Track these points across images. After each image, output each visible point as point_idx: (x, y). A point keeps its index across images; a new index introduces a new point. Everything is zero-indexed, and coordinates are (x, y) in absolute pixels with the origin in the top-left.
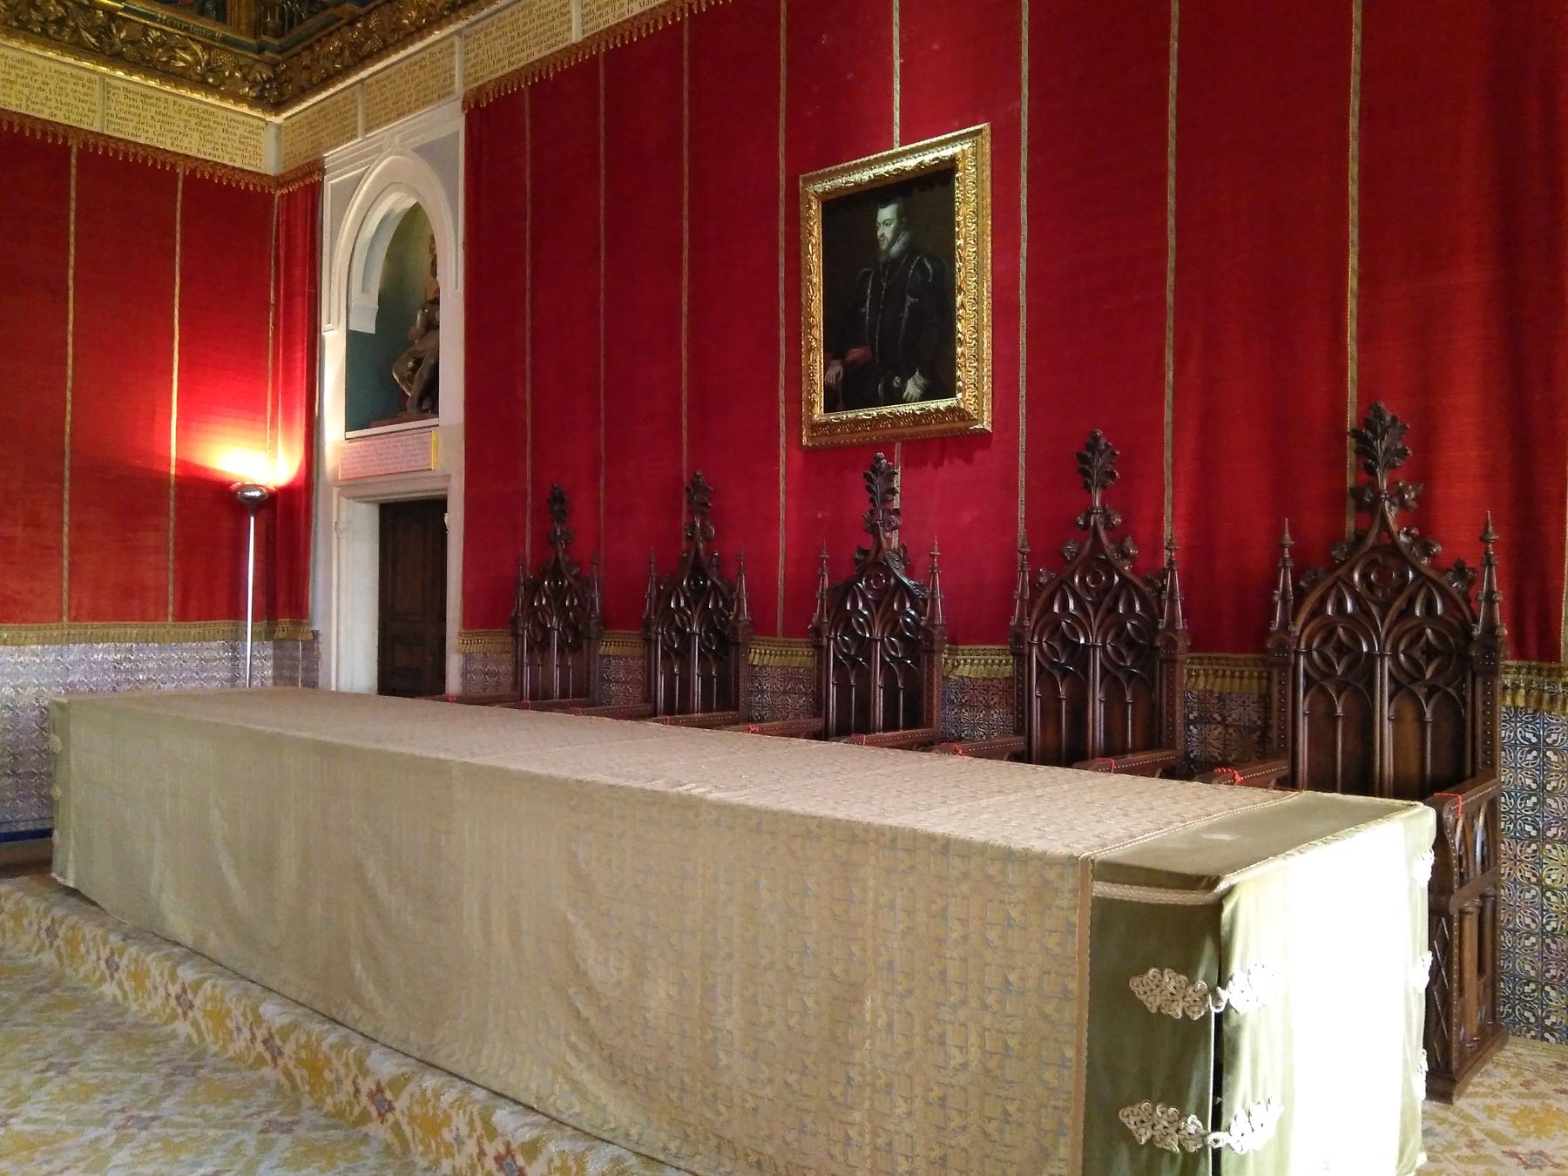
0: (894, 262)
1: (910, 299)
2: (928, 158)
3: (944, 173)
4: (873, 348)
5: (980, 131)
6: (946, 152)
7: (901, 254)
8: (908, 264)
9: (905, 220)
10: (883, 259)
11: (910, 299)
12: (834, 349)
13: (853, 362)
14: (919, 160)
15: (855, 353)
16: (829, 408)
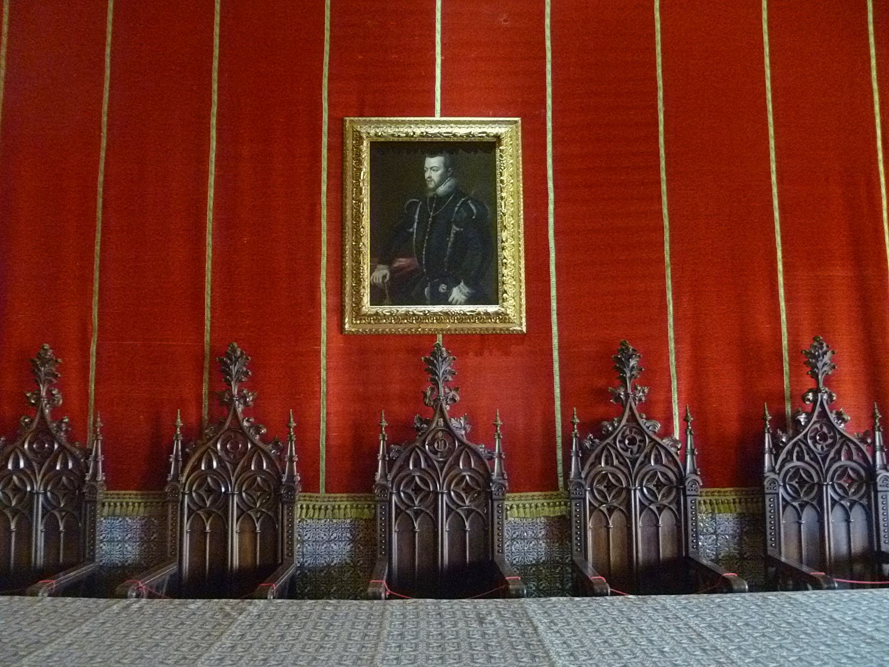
0: (440, 200)
1: (455, 229)
2: (476, 130)
3: (491, 145)
4: (420, 263)
5: (516, 122)
6: (493, 130)
7: (447, 195)
8: (455, 200)
9: (450, 169)
10: (431, 194)
11: (454, 227)
12: (380, 255)
13: (401, 269)
14: (468, 131)
15: (402, 262)
16: (373, 302)
